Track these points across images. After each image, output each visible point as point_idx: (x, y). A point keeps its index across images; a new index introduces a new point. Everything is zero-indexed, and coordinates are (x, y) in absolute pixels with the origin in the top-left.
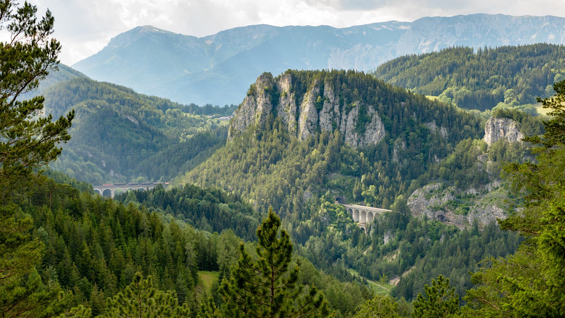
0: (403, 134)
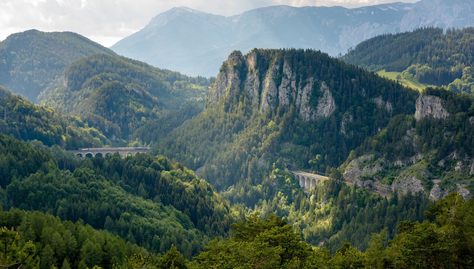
0: (351, 108)
